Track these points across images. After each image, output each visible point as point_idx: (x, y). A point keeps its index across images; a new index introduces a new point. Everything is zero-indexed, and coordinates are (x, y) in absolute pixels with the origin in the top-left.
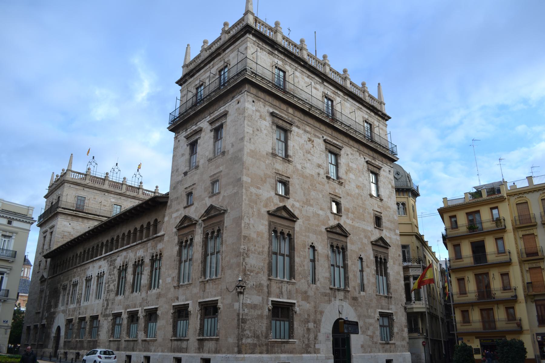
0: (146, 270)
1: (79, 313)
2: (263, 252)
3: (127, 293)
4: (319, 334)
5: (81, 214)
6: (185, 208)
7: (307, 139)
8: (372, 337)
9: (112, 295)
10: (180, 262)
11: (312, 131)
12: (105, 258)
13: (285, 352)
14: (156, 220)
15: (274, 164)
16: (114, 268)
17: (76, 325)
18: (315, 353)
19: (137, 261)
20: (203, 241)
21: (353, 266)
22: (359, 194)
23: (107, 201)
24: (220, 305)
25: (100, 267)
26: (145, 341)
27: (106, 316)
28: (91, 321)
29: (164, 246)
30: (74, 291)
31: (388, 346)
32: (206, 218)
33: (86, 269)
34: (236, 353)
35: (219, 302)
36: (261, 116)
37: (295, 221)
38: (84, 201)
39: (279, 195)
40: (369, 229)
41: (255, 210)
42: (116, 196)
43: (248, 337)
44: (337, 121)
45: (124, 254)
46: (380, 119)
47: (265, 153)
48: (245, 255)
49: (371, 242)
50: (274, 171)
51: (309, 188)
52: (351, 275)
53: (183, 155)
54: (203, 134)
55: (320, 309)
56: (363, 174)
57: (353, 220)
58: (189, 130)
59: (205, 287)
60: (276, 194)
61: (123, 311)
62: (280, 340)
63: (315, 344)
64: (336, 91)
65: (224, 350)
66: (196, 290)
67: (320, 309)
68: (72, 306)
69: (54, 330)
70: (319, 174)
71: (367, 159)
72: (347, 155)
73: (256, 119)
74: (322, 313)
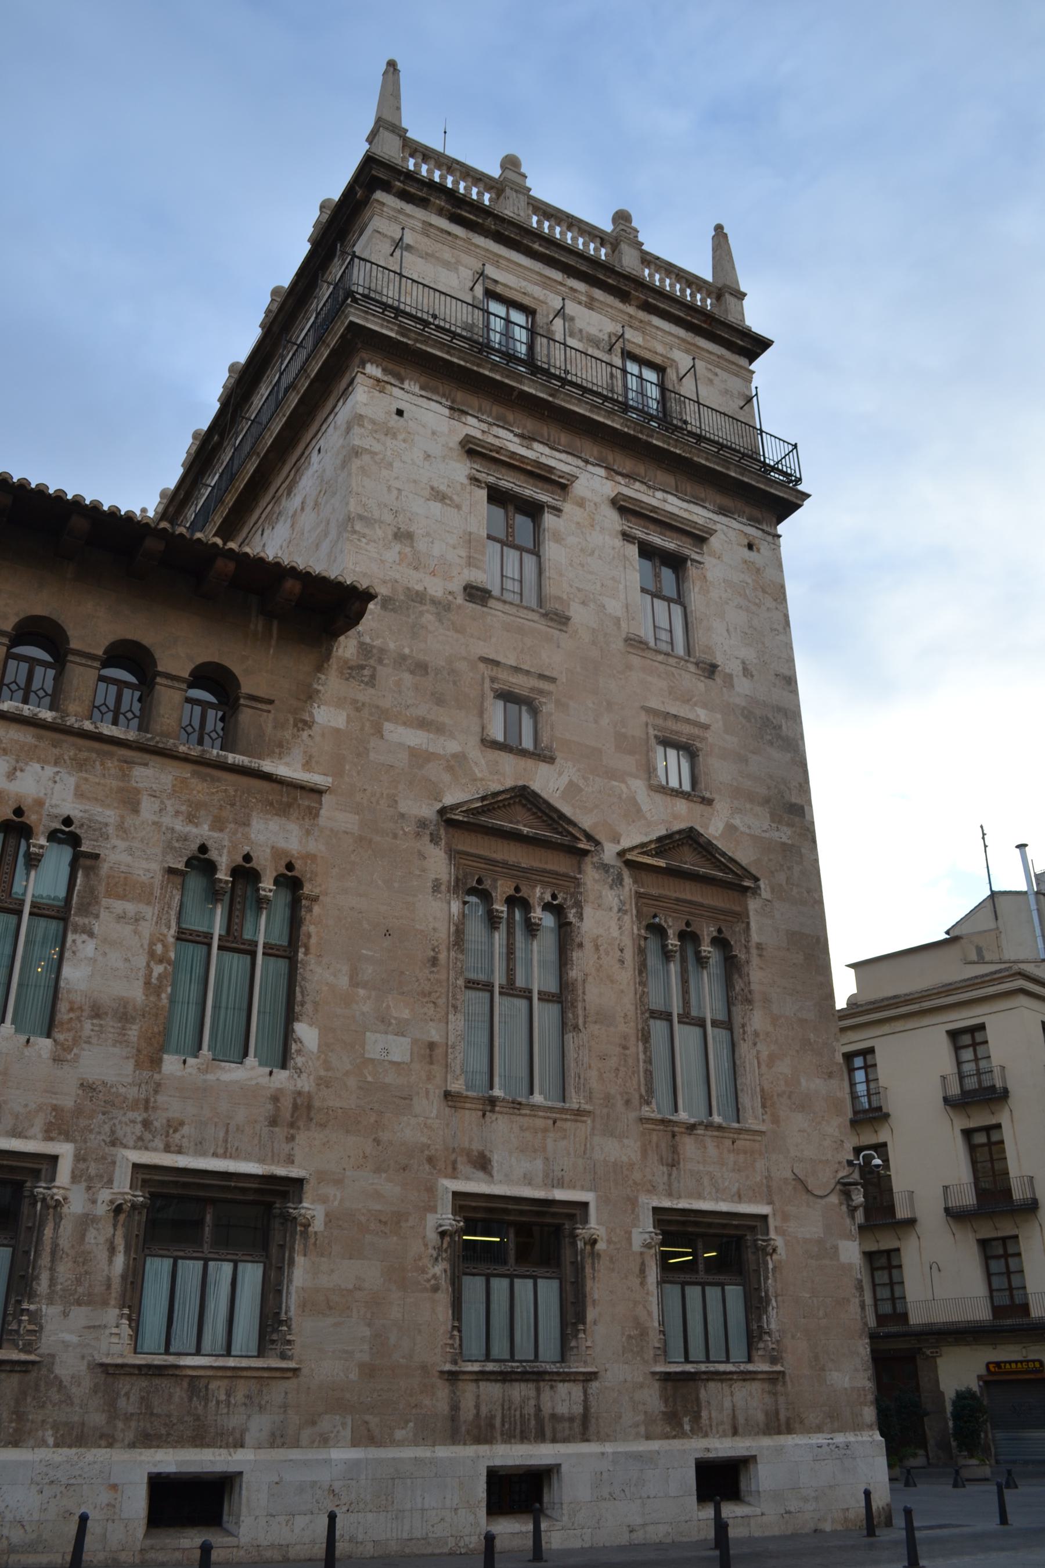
29: (314, 846)
32: (662, 863)
34: (870, 1427)
59: (674, 1149)
66: (621, 1149)
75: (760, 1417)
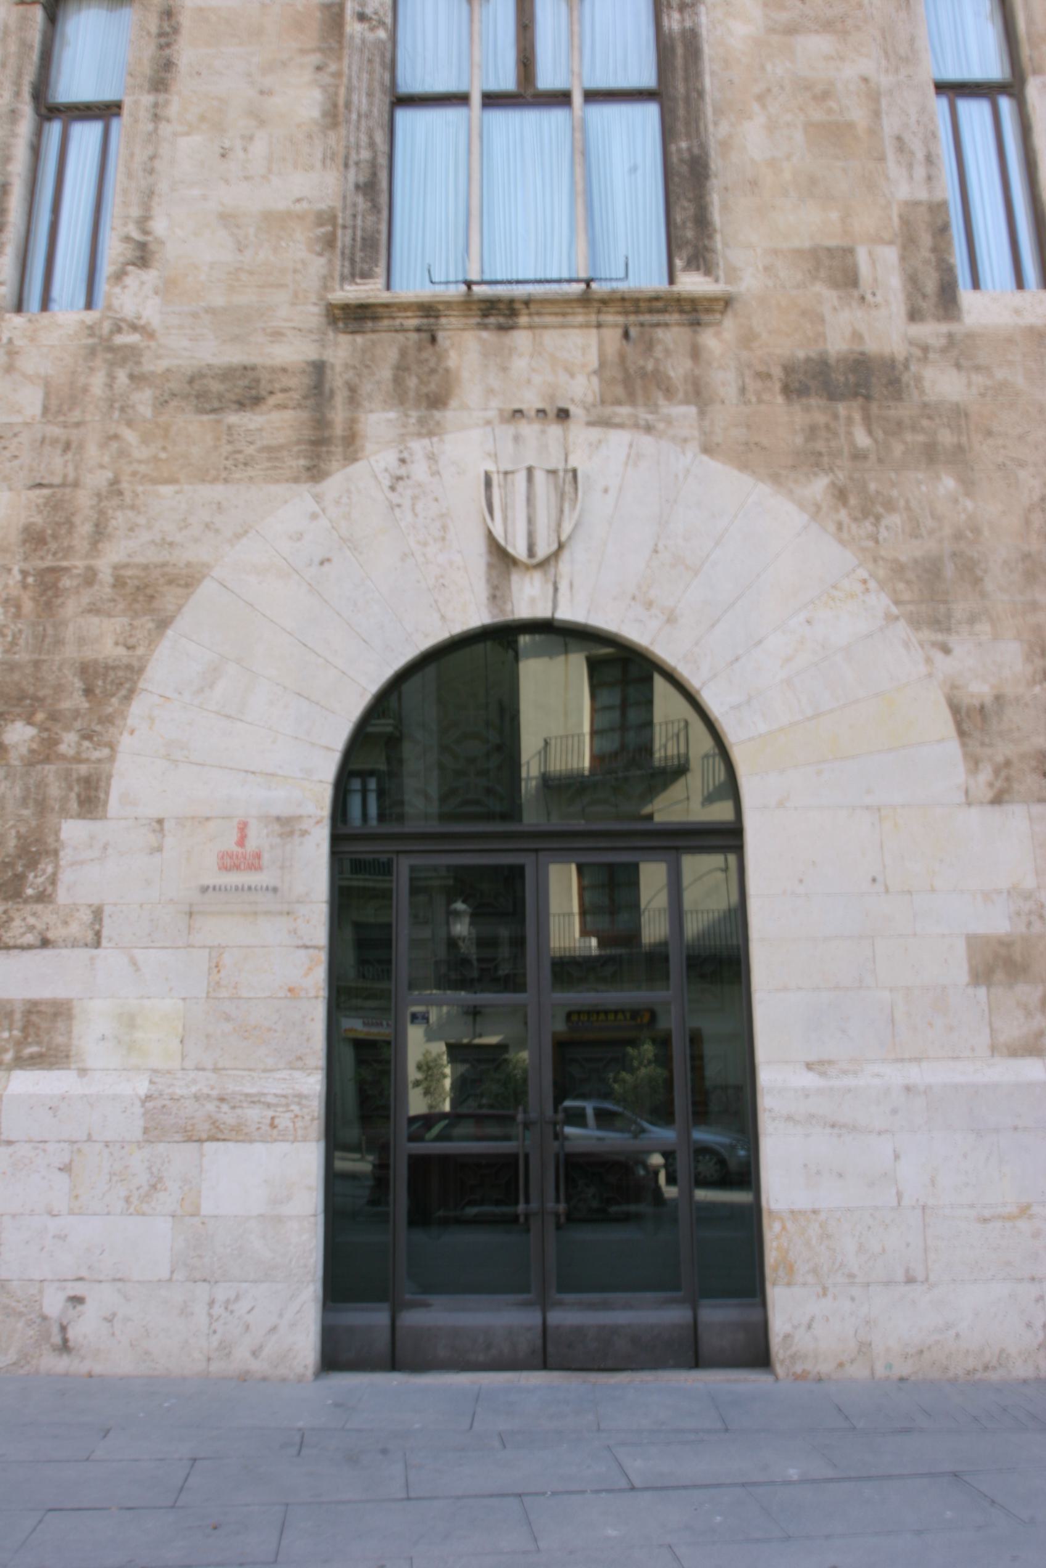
4: (73, 831)
21: (815, 45)
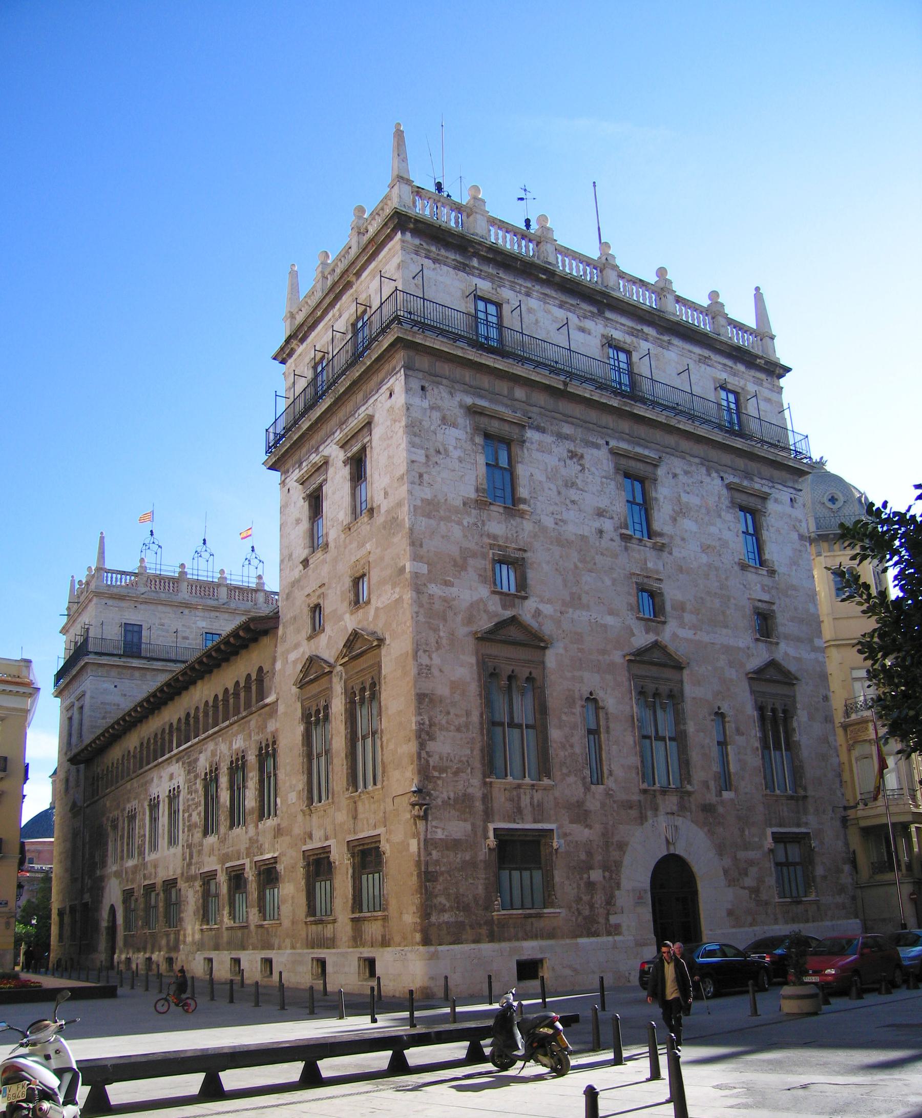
0: (252, 779)
1: (144, 875)
2: (467, 726)
3: (223, 829)
4: (617, 893)
5: (135, 663)
6: (310, 638)
7: (565, 454)
8: (755, 891)
9: (198, 834)
10: (309, 756)
11: (579, 433)
12: (178, 758)
13: (535, 937)
14: (260, 669)
15: (483, 524)
16: (196, 777)
17: (141, 900)
18: (609, 934)
19: (234, 759)
20: (346, 710)
21: (702, 734)
22: (709, 566)
23: (189, 627)
24: (385, 846)
25: (171, 777)
26: (261, 926)
27: (190, 879)
28: (165, 891)
29: (278, 725)
30: (131, 831)
31: (801, 908)
32: (346, 659)
33: (146, 783)
34: (418, 944)
35: (382, 839)
36: (444, 420)
37: (545, 648)
38: (140, 632)
39: (501, 593)
40: (741, 644)
41: (442, 634)
42: (207, 614)
43: (443, 910)
44: (643, 401)
45: (211, 746)
46: (762, 376)
47: (458, 503)
48: (424, 736)
49: (747, 674)
50: (486, 540)
51: (576, 567)
52: (695, 756)
53: (298, 521)
54: (331, 471)
55: (616, 838)
56: (720, 516)
57: (694, 627)
58: (304, 464)
59: (356, 809)
60: (494, 592)
61: (218, 867)
62: (520, 912)
63: (608, 914)
64: (639, 327)
65: (397, 939)
66: (342, 816)
67: (616, 838)
68: (130, 863)
69: (105, 914)
70: (601, 532)
71: (730, 479)
72: (675, 476)
73: (432, 428)
74: (622, 847)
75: (380, 938)
